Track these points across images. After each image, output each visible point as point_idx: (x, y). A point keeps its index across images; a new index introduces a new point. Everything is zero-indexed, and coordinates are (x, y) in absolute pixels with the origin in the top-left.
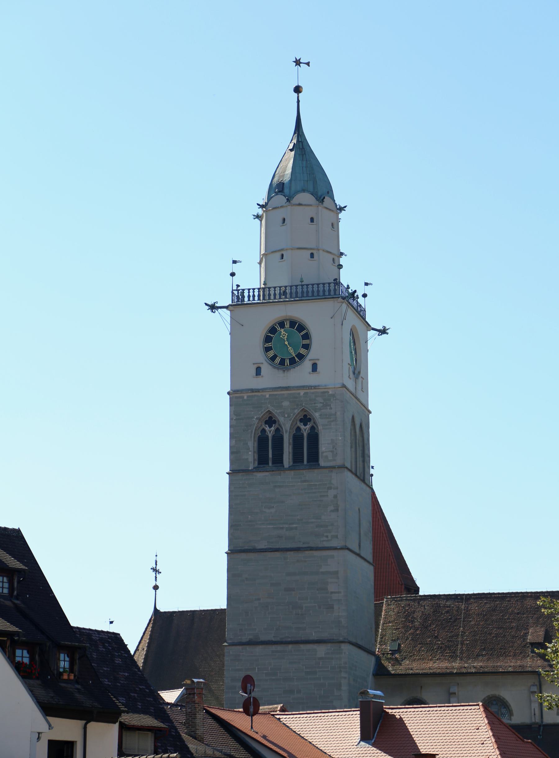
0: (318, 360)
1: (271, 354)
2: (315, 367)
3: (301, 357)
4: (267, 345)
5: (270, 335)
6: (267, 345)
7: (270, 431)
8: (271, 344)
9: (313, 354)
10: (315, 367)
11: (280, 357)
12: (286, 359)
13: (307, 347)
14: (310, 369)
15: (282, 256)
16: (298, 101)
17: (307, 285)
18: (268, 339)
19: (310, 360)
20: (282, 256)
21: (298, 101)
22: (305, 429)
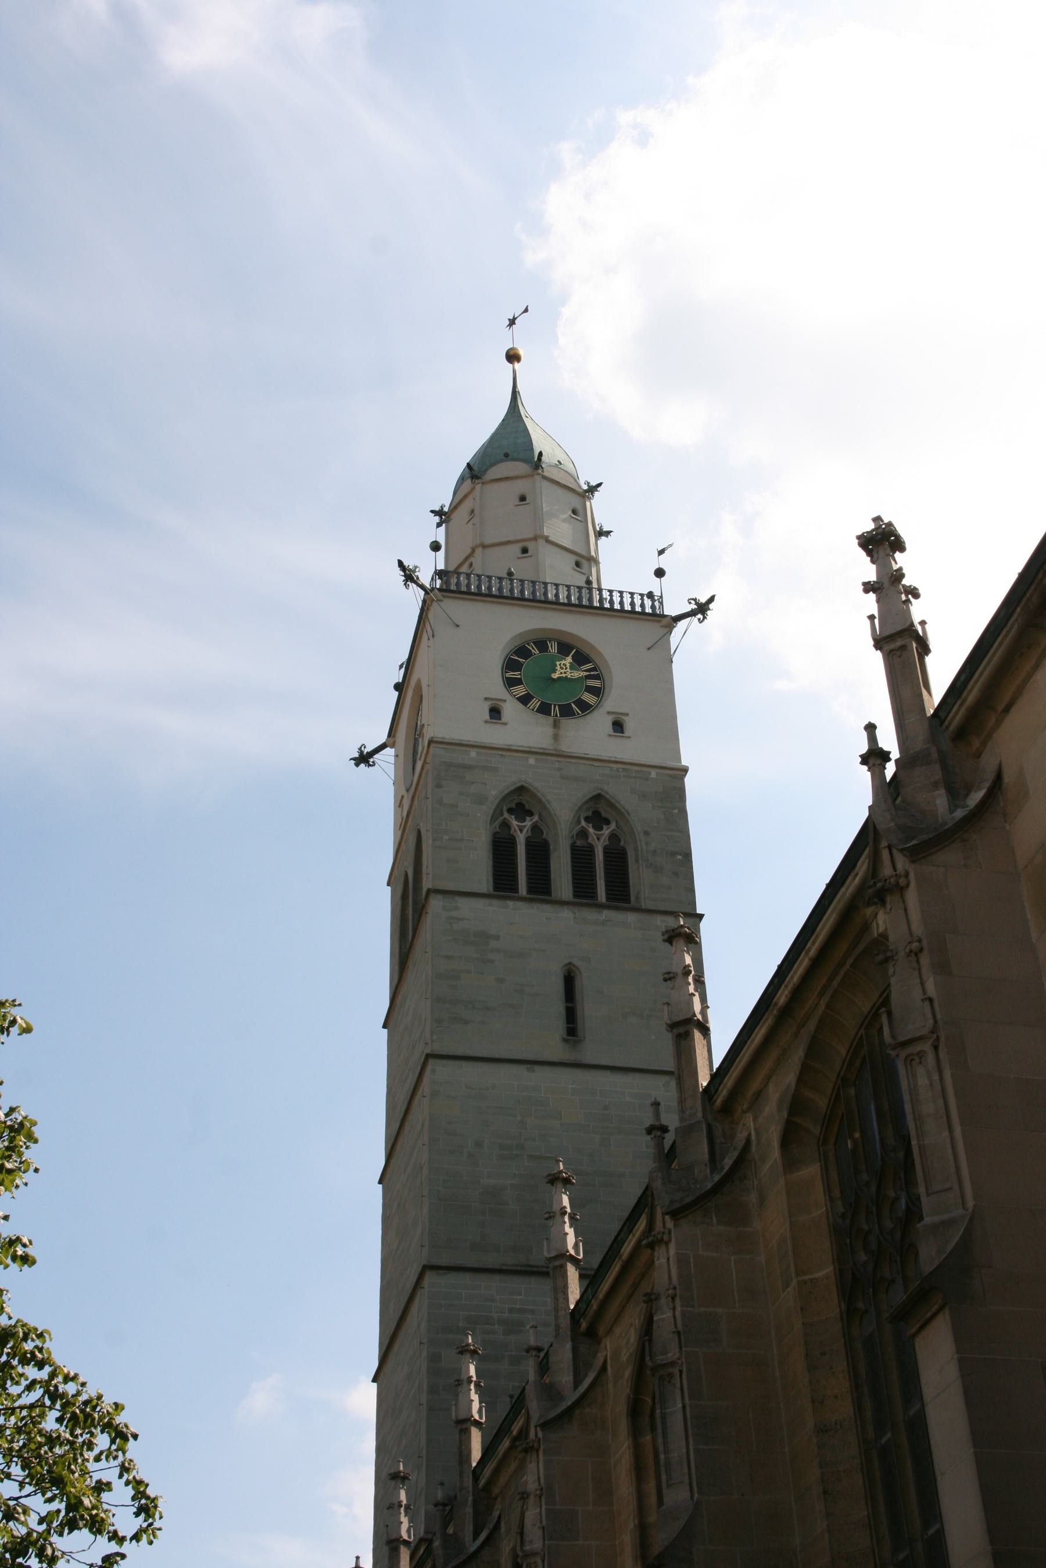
0: (627, 715)
1: (520, 690)
2: (618, 726)
3: (585, 707)
4: (510, 675)
5: (516, 658)
6: (510, 675)
8: (520, 674)
9: (612, 702)
10: (618, 726)
11: (539, 700)
12: (553, 706)
13: (597, 692)
14: (609, 728)
15: (525, 551)
18: (510, 665)
19: (609, 713)
20: (525, 551)
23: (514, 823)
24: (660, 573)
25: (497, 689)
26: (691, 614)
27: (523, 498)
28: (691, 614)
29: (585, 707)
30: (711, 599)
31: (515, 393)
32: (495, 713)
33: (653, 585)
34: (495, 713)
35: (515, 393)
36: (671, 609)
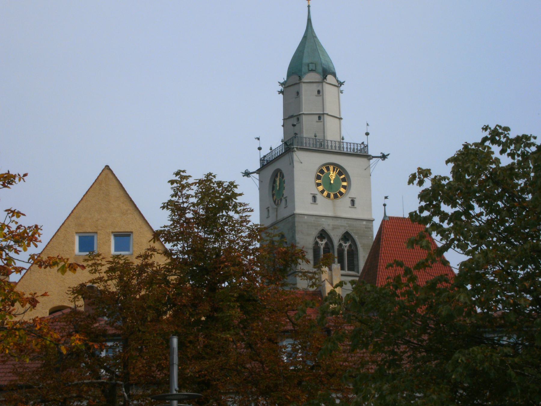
2: (353, 202)
7: (322, 243)
9: (353, 193)
10: (353, 202)
14: (349, 203)
15: (320, 118)
16: (309, 6)
17: (347, 143)
18: (318, 177)
19: (350, 198)
21: (309, 6)
22: (346, 246)
23: (320, 242)
24: (367, 134)
25: (315, 191)
26: (380, 157)
27: (319, 92)
28: (380, 157)
29: (341, 194)
30: (388, 155)
31: (309, 20)
32: (314, 198)
33: (364, 139)
34: (314, 198)
35: (309, 20)
36: (371, 152)
